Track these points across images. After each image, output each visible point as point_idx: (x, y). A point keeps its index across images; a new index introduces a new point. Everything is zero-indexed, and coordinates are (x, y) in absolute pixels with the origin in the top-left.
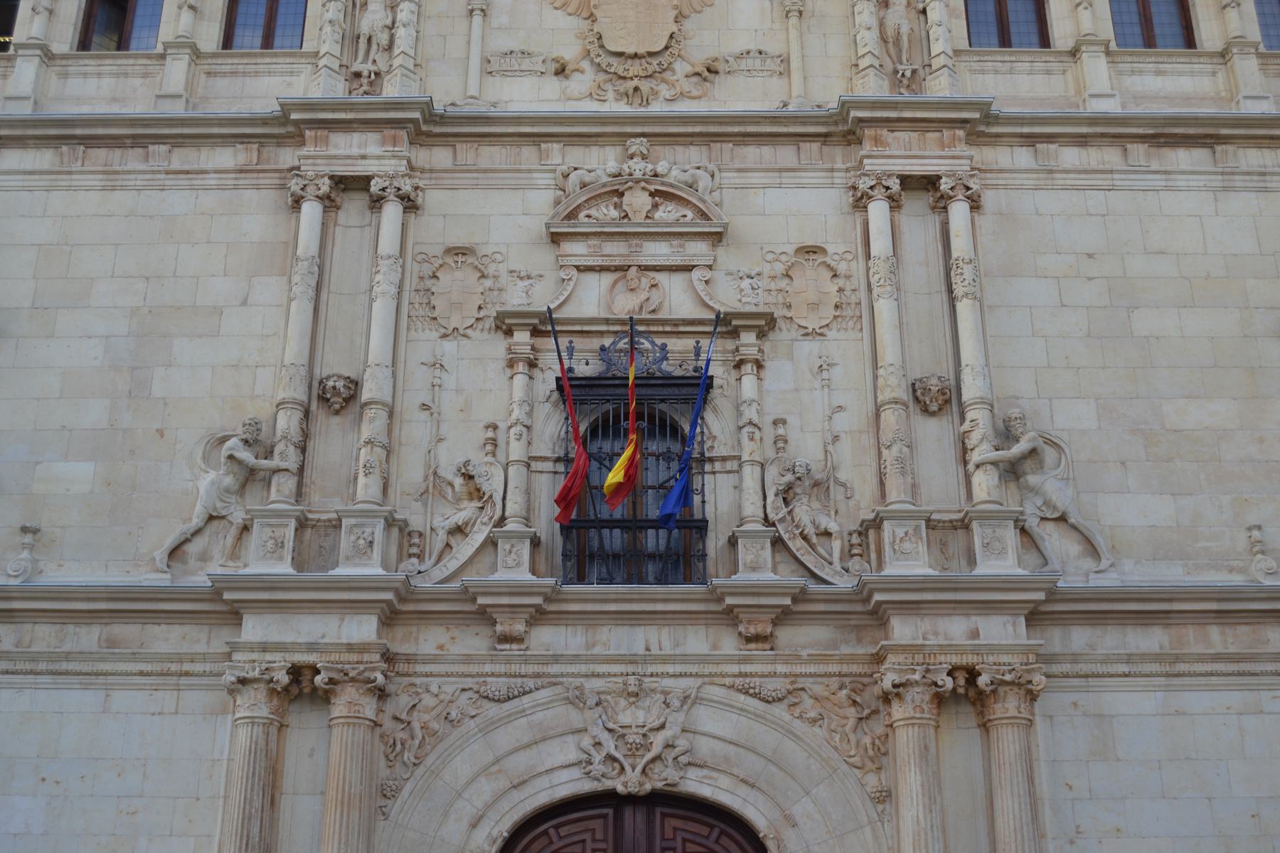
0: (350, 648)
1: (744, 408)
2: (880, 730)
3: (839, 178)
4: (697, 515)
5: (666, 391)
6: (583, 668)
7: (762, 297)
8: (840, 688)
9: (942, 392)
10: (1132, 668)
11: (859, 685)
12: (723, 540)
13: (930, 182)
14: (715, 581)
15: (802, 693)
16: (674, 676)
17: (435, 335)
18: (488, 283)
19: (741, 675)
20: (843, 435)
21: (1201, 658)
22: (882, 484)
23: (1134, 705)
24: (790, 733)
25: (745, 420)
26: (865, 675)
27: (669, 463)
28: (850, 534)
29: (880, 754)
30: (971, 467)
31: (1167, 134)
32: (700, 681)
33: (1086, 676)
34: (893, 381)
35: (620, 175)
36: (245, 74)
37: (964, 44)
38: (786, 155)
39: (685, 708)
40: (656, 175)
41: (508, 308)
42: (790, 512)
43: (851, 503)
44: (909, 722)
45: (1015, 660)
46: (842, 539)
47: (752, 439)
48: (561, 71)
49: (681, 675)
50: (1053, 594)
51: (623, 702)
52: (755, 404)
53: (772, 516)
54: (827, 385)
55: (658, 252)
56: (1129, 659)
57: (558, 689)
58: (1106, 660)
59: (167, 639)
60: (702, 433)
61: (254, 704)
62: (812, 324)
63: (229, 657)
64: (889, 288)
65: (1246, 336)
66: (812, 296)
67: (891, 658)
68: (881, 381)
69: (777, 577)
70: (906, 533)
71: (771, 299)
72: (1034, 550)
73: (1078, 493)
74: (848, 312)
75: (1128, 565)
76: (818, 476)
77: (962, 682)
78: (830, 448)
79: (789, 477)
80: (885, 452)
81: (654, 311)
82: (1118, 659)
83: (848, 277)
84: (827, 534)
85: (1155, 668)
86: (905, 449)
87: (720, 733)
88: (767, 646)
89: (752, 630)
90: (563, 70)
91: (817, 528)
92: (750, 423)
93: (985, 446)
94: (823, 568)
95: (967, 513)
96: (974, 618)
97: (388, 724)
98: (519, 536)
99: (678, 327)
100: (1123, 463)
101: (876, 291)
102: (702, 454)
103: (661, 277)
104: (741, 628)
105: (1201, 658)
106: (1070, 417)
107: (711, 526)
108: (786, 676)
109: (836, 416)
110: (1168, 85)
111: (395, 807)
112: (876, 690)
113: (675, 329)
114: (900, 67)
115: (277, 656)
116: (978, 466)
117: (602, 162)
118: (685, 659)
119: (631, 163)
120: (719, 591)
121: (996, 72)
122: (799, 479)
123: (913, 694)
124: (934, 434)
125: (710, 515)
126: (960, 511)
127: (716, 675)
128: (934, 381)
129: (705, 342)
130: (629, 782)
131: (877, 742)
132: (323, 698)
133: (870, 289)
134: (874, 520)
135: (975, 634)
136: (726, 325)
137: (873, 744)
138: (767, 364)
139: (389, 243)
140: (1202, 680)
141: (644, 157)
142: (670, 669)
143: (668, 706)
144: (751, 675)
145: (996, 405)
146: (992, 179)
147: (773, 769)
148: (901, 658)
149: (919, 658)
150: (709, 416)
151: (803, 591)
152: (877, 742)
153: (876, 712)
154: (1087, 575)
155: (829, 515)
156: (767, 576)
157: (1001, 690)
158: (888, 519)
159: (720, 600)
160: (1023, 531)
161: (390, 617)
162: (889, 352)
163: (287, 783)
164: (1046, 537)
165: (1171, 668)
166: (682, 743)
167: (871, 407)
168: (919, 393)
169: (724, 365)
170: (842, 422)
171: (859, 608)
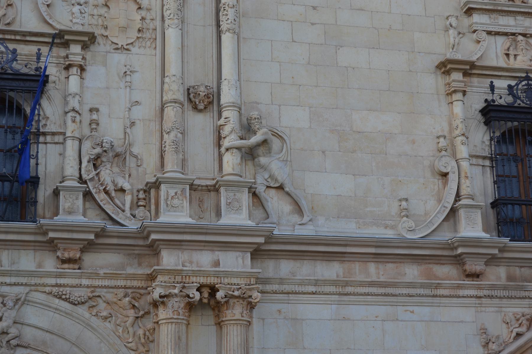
1: (70, 99)
2: (150, 325)
4: (33, 174)
5: (15, 84)
7: (88, 19)
8: (125, 297)
9: (207, 96)
10: (318, 289)
11: (137, 294)
12: (50, 191)
14: (42, 221)
15: (98, 299)
16: (10, 285)
19: (57, 285)
20: (138, 122)
21: (362, 284)
22: (162, 157)
23: (316, 312)
24: (89, 326)
25: (70, 107)
26: (142, 288)
27: (14, 135)
28: (138, 191)
30: (223, 150)
32: (28, 289)
33: (288, 293)
34: (175, 87)
39: (17, 307)
42: (97, 174)
43: (140, 169)
44: (170, 321)
45: (242, 282)
46: (132, 194)
47: (74, 121)
49: (15, 284)
50: (270, 239)
52: (78, 97)
53: (85, 176)
54: (130, 86)
56: (316, 283)
58: (302, 283)
60: (39, 115)
62: (121, 41)
64: (176, 21)
65: (410, 71)
66: (122, 22)
67: (160, 278)
68: (166, 86)
69: (86, 220)
70: (176, 193)
71: (94, 22)
72: (261, 208)
73: (293, 171)
74: (147, 35)
75: (321, 220)
76: (119, 150)
77: (206, 295)
78: (128, 130)
79: (98, 150)
80: (166, 136)
81: (8, 24)
82: (310, 283)
83: (149, 10)
84: (122, 190)
85: (333, 289)
86: (179, 135)
87: (40, 325)
88: (76, 266)
89: (66, 255)
91: (116, 186)
92: (74, 110)
93: (233, 136)
94: (118, 214)
95: (217, 182)
96: (217, 253)
99: (25, 37)
100: (323, 152)
101: (167, 22)
102: (39, 130)
104: (59, 254)
105: (362, 284)
106: (292, 119)
107: (41, 181)
108: (88, 287)
109: (134, 108)
112: (149, 298)
113: (23, 38)
116: (227, 150)
118: (19, 273)
120: (44, 228)
122: (105, 151)
123: (173, 303)
124: (200, 124)
125: (41, 174)
126: (213, 179)
127: (39, 285)
128: (202, 89)
129: (45, 50)
131: (147, 333)
134: (155, 183)
135: (217, 264)
136: (60, 39)
137: (145, 334)
138: (88, 68)
140: (361, 298)
142: (8, 280)
143: (5, 305)
144: (64, 286)
145: (243, 108)
147: (76, 349)
148: (166, 278)
149: (178, 279)
150: (44, 102)
151: (103, 230)
152: (147, 333)
153: (148, 313)
154: (294, 226)
155: (124, 177)
156: (78, 219)
157: (231, 301)
158: (165, 183)
159: (45, 233)
160: (255, 195)
162: (173, 68)
164: (269, 200)
165: (343, 289)
166: (13, 331)
167: (158, 103)
168: (192, 96)
169: (57, 66)
170: (137, 113)
171: (141, 242)
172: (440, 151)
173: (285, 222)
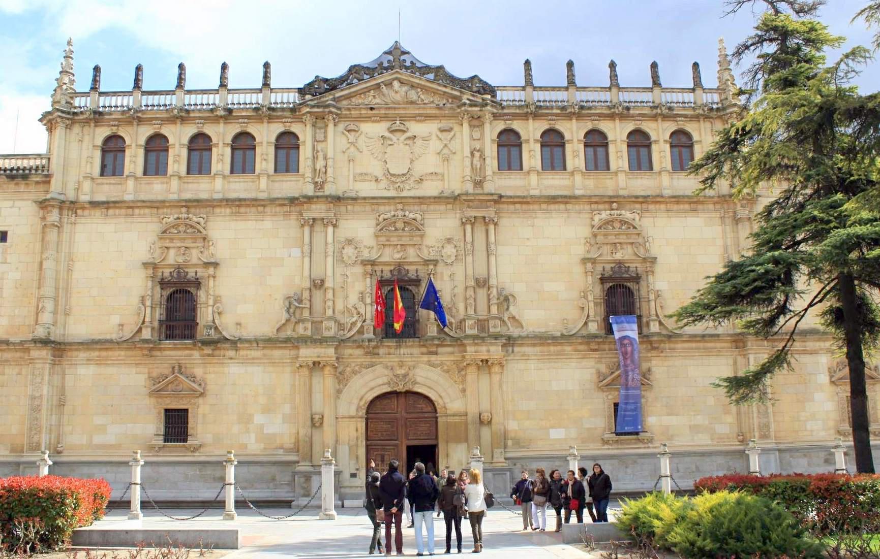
3: (458, 215)
13: (484, 218)
29: (464, 381)
31: (553, 200)
37: (496, 169)
38: (443, 207)
41: (364, 258)
48: (377, 180)
55: (405, 241)
59: (277, 353)
61: (305, 371)
62: (449, 261)
63: (297, 357)
74: (459, 257)
99: (411, 263)
103: (408, 247)
106: (518, 289)
110: (555, 183)
111: (341, 396)
117: (388, 211)
124: (482, 293)
130: (400, 388)
135: (488, 351)
139: (330, 239)
146: (501, 215)
162: (470, 271)
163: (314, 390)
170: (456, 291)
173: (515, 332)
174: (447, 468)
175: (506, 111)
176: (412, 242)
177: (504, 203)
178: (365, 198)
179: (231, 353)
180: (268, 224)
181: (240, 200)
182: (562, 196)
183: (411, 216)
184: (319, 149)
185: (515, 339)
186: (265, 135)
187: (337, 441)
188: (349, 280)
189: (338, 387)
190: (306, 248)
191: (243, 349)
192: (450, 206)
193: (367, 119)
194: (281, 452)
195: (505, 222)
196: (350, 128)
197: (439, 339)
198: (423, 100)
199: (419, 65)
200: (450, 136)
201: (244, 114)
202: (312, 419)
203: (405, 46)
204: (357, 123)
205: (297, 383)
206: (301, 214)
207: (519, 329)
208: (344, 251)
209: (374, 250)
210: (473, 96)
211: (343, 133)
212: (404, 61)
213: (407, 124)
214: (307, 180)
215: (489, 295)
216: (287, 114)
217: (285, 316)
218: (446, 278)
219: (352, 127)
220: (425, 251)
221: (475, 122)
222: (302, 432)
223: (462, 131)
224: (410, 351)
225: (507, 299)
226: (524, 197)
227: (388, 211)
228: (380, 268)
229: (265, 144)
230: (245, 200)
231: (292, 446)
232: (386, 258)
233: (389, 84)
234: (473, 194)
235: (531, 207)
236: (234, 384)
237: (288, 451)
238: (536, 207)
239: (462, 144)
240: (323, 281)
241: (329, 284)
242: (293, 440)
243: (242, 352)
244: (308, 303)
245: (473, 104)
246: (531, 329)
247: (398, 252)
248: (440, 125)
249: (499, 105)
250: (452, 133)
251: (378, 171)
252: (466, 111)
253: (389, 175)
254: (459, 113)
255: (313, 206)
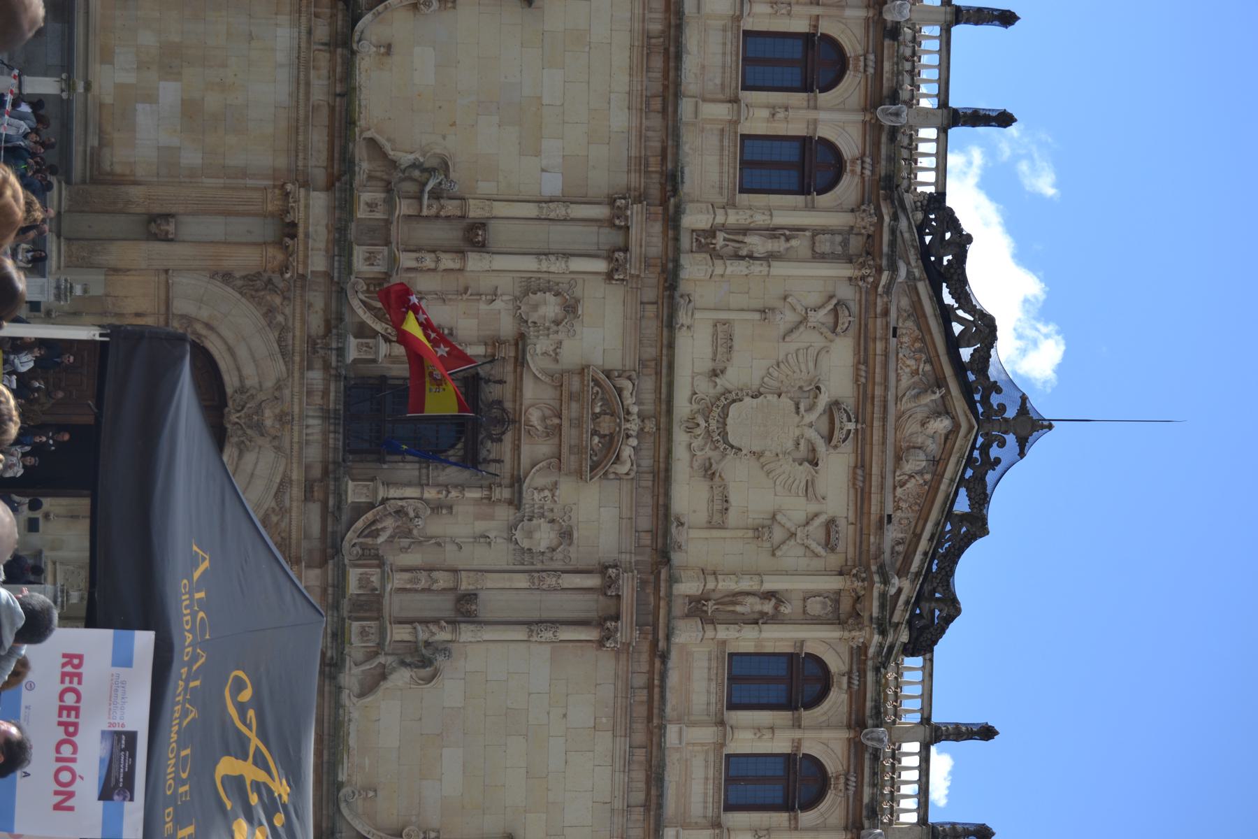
0: (306, 257)
6: (296, 389)
9: (468, 611)
13: (617, 618)
17: (518, 294)
18: (554, 328)
31: (655, 777)
35: (628, 413)
36: (721, 156)
38: (645, 522)
40: (628, 436)
48: (715, 373)
51: (277, 411)
57: (285, 375)
59: (318, 139)
62: (518, 535)
63: (306, 185)
74: (527, 557)
78: (433, 541)
79: (412, 514)
90: (716, 376)
97: (266, 276)
98: (377, 353)
99: (517, 448)
103: (556, 440)
106: (451, 687)
114: (710, 603)
115: (302, 215)
119: (637, 421)
121: (709, 669)
124: (444, 606)
128: (474, 607)
132: (279, 244)
133: (538, 572)
136: (517, 481)
141: (642, 429)
146: (623, 657)
161: (328, 275)
162: (492, 581)
167: (461, 567)
170: (450, 548)
172: (425, 833)
173: (351, 677)
174: (47, 516)
175: (870, 676)
176: (565, 450)
177: (652, 664)
178: (671, 346)
179: (322, 31)
180: (620, 119)
181: (678, 57)
182: (661, 796)
183: (627, 452)
184: (794, 243)
185: (333, 678)
186: (836, 118)
187: (116, 270)
188: (483, 307)
189: (237, 275)
190: (559, 211)
191: (332, 60)
192: (646, 540)
193: (863, 359)
194: (94, 141)
195: (605, 666)
196: (843, 314)
197: (339, 507)
198: (902, 484)
199: (990, 476)
200: (814, 545)
201: (887, 66)
202: (167, 216)
203: (1041, 446)
204: (853, 331)
205: (250, 182)
206: (638, 199)
207: (356, 689)
208: (549, 297)
209: (552, 366)
210: (907, 603)
211: (831, 297)
212: (1002, 444)
213: (848, 446)
214: (720, 212)
215: (436, 621)
216: (883, 168)
217: (406, 159)
218: (480, 526)
219: (844, 319)
220: (540, 481)
221: (846, 605)
222: (135, 192)
223: (825, 572)
224: (312, 437)
225: (425, 662)
226: (662, 710)
227: (637, 398)
228: (510, 378)
229: (812, 115)
230: (678, 68)
231: (107, 167)
232: (530, 391)
233: (944, 410)
234: (669, 594)
235: (640, 726)
236: (251, 37)
237: (94, 158)
238: (640, 737)
239: (795, 573)
240: (481, 247)
241: (475, 262)
242: (118, 169)
243: (323, 58)
244: (433, 211)
245: (888, 603)
246: (355, 715)
247: (544, 418)
248: (842, 523)
249: (886, 658)
250: (820, 550)
251: (733, 377)
252: (872, 584)
253: (729, 399)
254: (868, 568)
255: (657, 228)
